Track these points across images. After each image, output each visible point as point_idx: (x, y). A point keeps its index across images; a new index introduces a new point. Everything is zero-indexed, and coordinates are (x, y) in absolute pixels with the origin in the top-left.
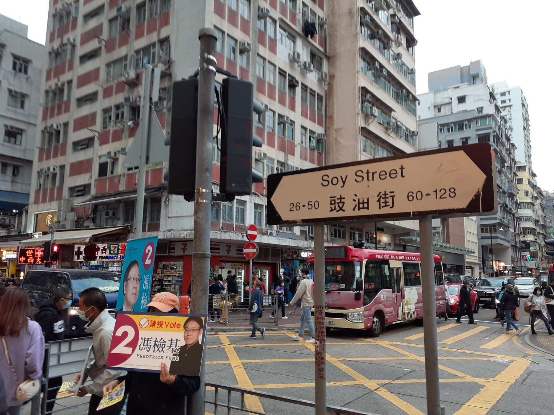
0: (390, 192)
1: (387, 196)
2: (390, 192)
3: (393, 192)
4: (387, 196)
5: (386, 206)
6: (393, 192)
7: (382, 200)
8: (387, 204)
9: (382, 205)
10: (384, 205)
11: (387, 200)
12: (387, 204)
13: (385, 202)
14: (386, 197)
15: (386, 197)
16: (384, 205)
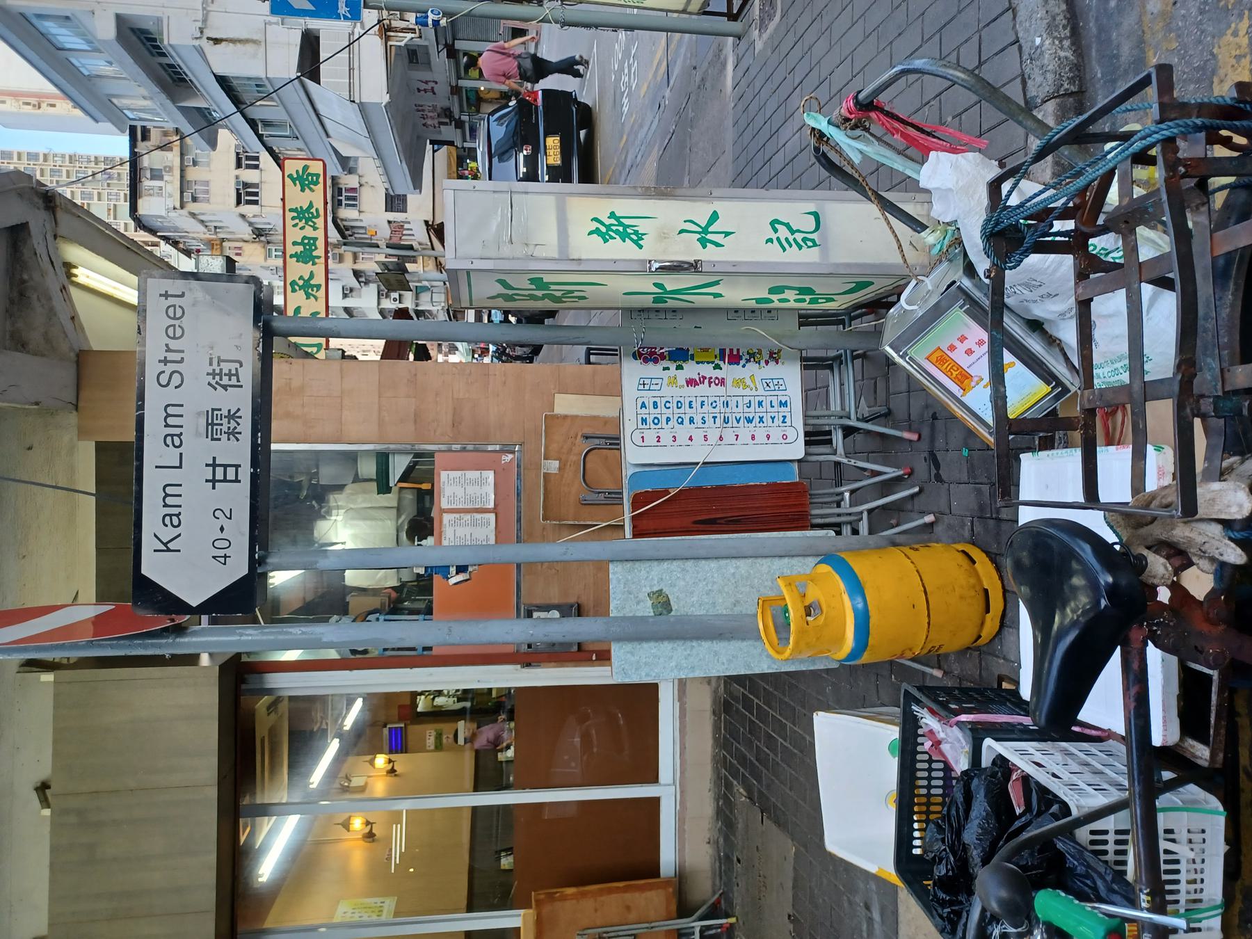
0: (211, 364)
1: (217, 371)
2: (211, 364)
3: (211, 359)
4: (217, 371)
5: (237, 375)
6: (211, 359)
7: (225, 381)
8: (233, 372)
9: (234, 381)
10: (234, 378)
11: (225, 371)
12: (233, 372)
13: (230, 375)
14: (220, 374)
15: (220, 374)
16: (234, 378)
